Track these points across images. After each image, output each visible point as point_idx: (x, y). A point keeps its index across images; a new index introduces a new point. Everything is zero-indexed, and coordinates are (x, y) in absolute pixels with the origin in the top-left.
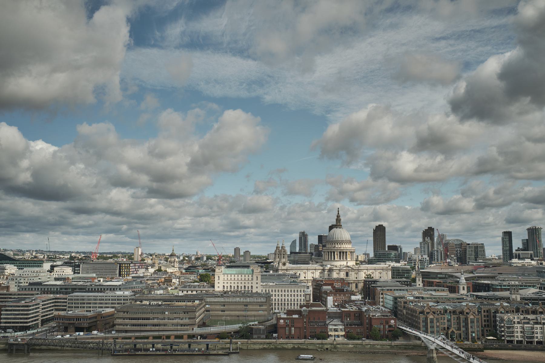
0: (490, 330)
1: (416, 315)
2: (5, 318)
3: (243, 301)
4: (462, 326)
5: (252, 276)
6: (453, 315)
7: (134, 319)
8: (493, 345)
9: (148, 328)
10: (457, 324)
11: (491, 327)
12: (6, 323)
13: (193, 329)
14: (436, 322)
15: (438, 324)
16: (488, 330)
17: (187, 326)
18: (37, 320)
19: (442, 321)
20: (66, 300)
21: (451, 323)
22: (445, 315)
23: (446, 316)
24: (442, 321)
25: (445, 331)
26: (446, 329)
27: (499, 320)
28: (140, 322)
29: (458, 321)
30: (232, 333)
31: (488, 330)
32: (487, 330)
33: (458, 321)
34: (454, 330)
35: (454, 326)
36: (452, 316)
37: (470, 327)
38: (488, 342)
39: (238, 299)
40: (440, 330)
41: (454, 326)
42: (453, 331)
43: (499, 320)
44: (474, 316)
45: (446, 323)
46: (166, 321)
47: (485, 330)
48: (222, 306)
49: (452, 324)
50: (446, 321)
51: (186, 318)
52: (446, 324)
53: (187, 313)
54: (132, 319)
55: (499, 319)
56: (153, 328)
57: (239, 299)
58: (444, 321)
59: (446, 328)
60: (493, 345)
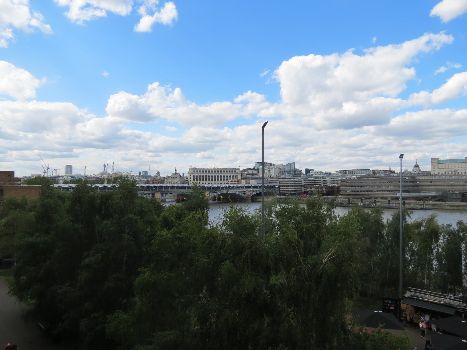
2: (283, 188)
3: (448, 178)
5: (465, 164)
7: (353, 187)
9: (362, 193)
12: (283, 191)
13: (397, 195)
17: (392, 192)
18: (301, 191)
20: (320, 181)
28: (357, 188)
30: (430, 197)
39: (443, 177)
46: (376, 188)
48: (429, 183)
51: (391, 186)
53: (392, 182)
54: (351, 187)
56: (366, 193)
57: (445, 177)
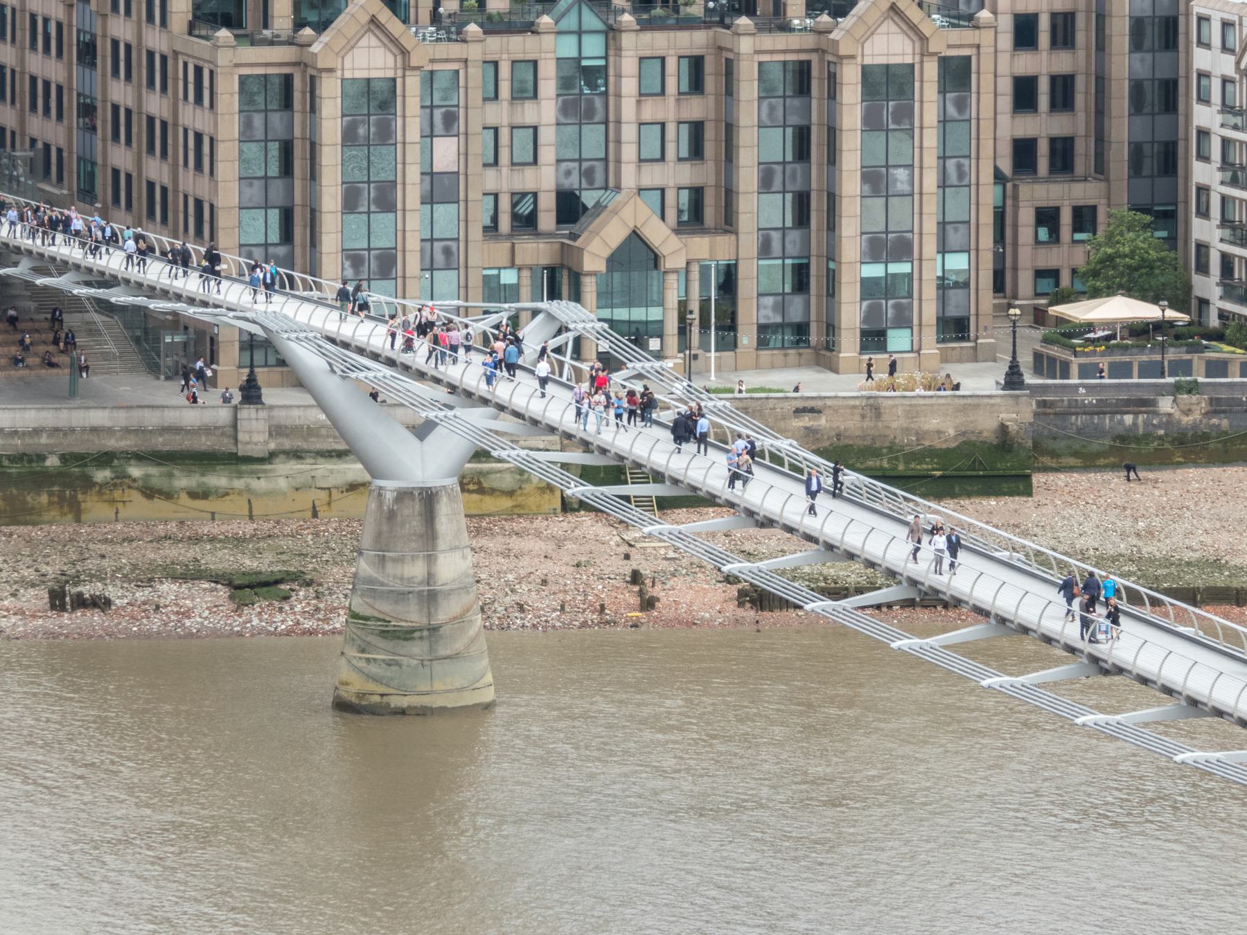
0: (1084, 218)
1: (155, 40)
4: (747, 177)
6: (647, 26)
8: (1143, 404)
10: (684, 153)
11: (1101, 168)
14: (430, 135)
15: (446, 153)
16: (1066, 218)
19: (499, 114)
21: (611, 140)
22: (530, 28)
23: (548, 40)
24: (499, 114)
25: (535, 251)
26: (547, 220)
27: (1230, 71)
29: (696, 108)
31: (1066, 218)
32: (1047, 217)
33: (696, 108)
34: (659, 234)
35: (654, 176)
36: (627, 40)
37: (851, 185)
38: (1085, 372)
40: (476, 233)
41: (654, 176)
42: (636, 236)
43: (1230, 71)
44: (913, 29)
45: (547, 135)
47: (1027, 216)
49: (629, 152)
50: (545, 110)
52: (547, 154)
55: (1225, 65)
58: (528, 113)
59: (548, 203)
60: (1143, 404)
